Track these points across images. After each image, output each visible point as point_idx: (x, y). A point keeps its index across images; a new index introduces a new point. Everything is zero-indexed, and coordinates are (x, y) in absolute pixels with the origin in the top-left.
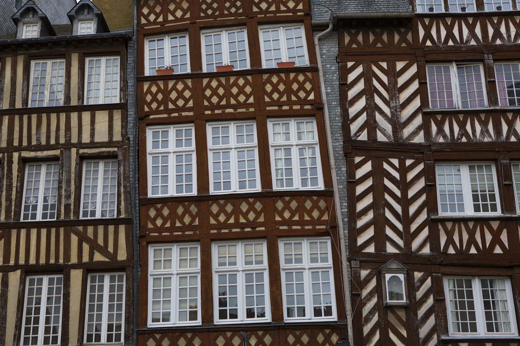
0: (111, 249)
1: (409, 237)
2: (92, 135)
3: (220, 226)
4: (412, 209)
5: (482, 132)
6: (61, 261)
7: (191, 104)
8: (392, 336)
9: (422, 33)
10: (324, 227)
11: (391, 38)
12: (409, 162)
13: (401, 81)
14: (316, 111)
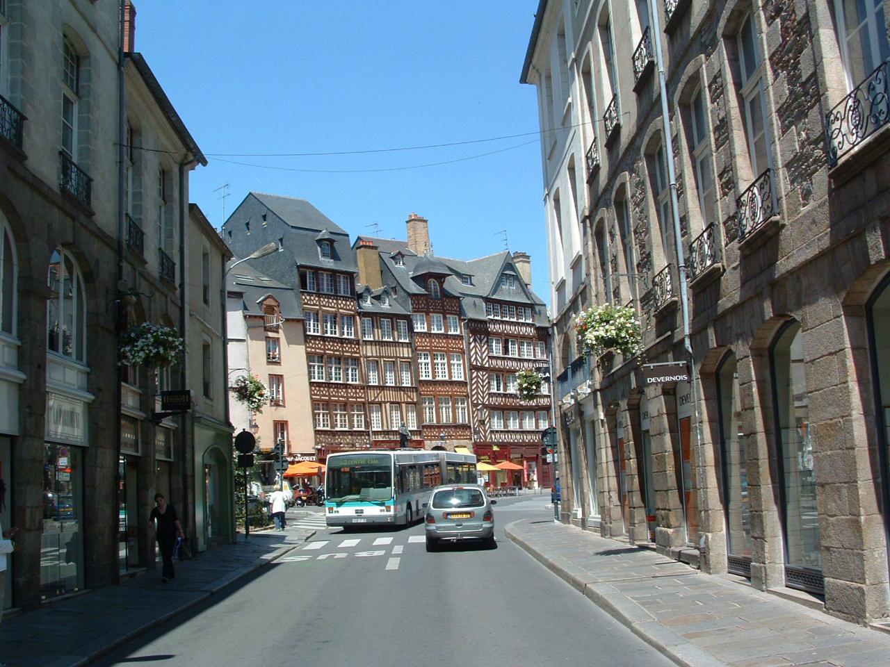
1: (483, 398)
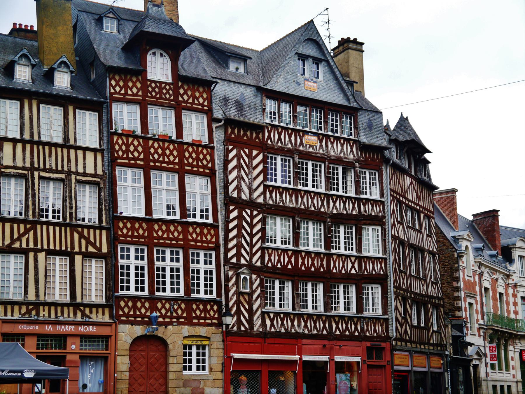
1: (252, 255)
2: (84, 168)
3: (159, 238)
4: (255, 240)
6: (69, 249)
7: (142, 156)
8: (242, 308)
9: (267, 134)
10: (213, 245)
11: (252, 134)
13: (255, 162)
14: (211, 174)
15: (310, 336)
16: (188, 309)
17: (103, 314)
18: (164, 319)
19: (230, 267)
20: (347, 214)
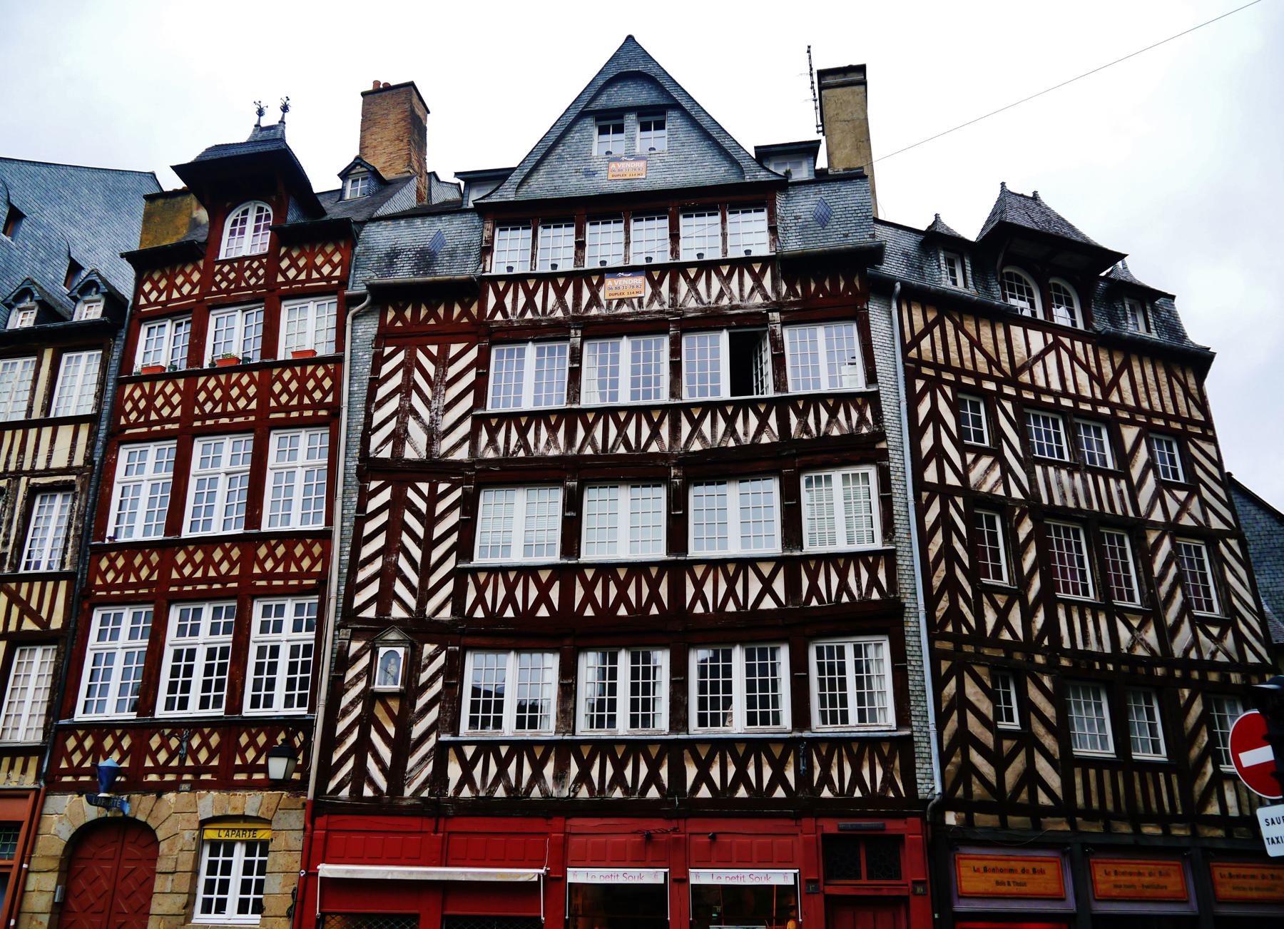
0: (44, 614)
1: (424, 594)
2: (49, 459)
4: (436, 555)
5: (548, 443)
7: (178, 413)
9: (492, 301)
10: (313, 582)
11: (449, 311)
12: (442, 487)
13: (452, 371)
15: (599, 807)
16: (228, 748)
17: (24, 771)
18: (162, 776)
19: (354, 630)
20: (740, 448)
